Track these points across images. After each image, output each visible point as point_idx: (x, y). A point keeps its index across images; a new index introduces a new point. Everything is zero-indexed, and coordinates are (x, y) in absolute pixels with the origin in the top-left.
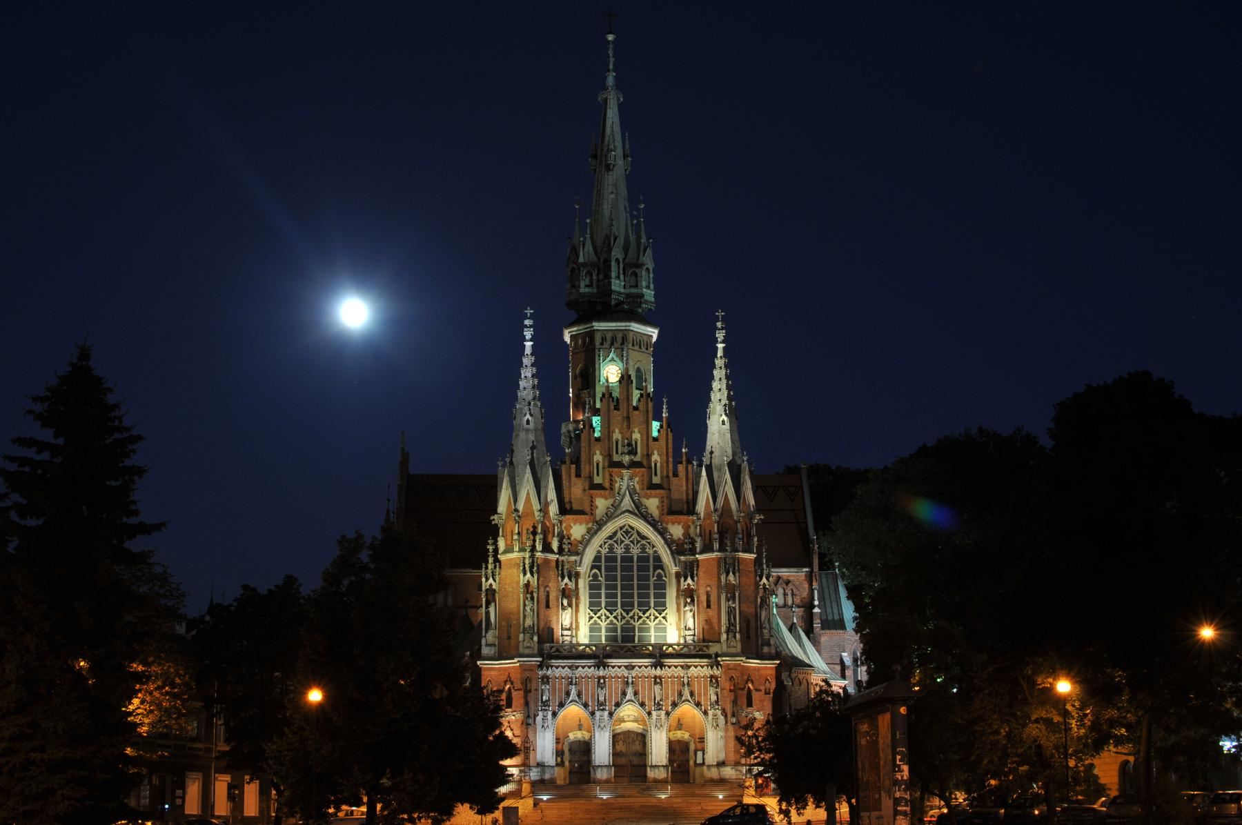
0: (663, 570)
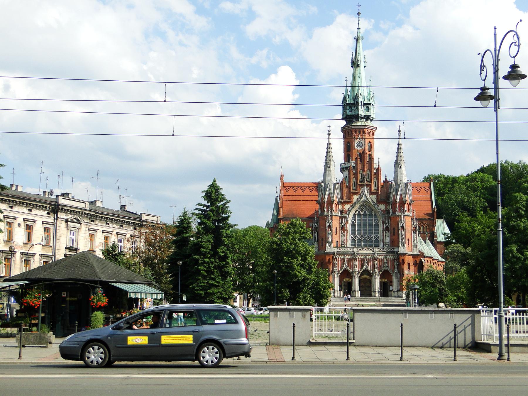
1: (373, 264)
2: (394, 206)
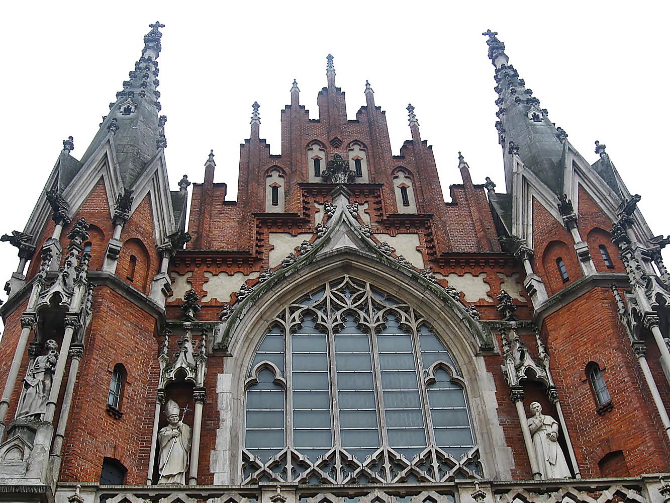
2: (553, 256)
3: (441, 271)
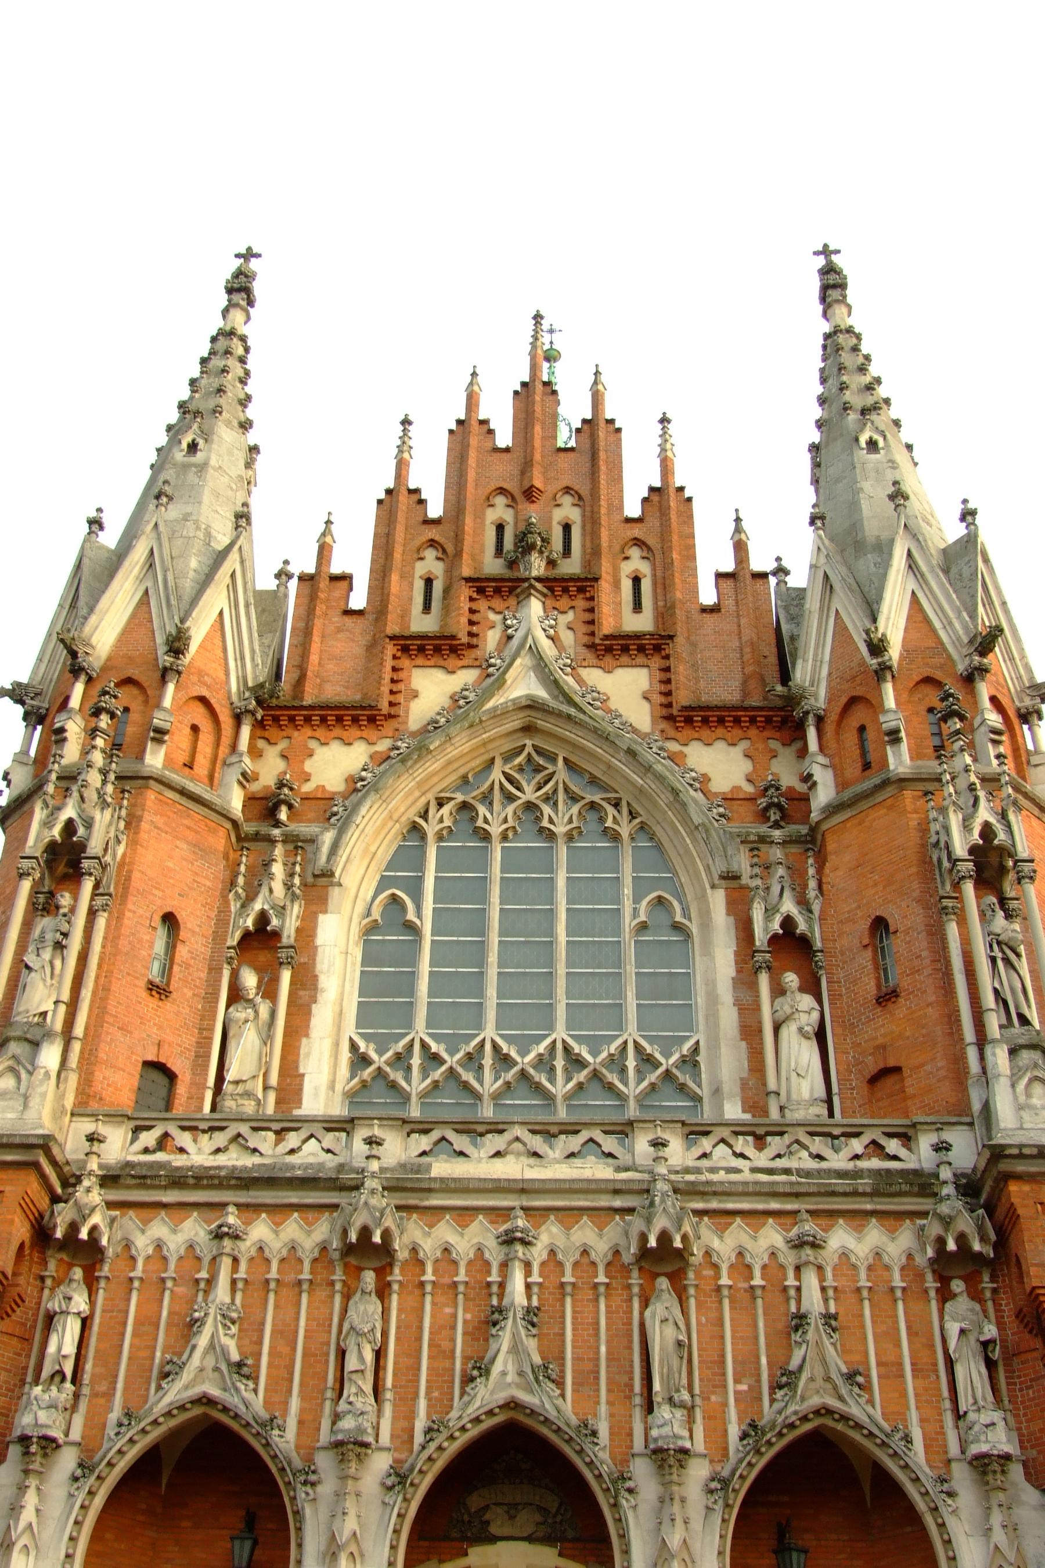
0: (681, 903)
1: (620, 1335)
3: (679, 735)
